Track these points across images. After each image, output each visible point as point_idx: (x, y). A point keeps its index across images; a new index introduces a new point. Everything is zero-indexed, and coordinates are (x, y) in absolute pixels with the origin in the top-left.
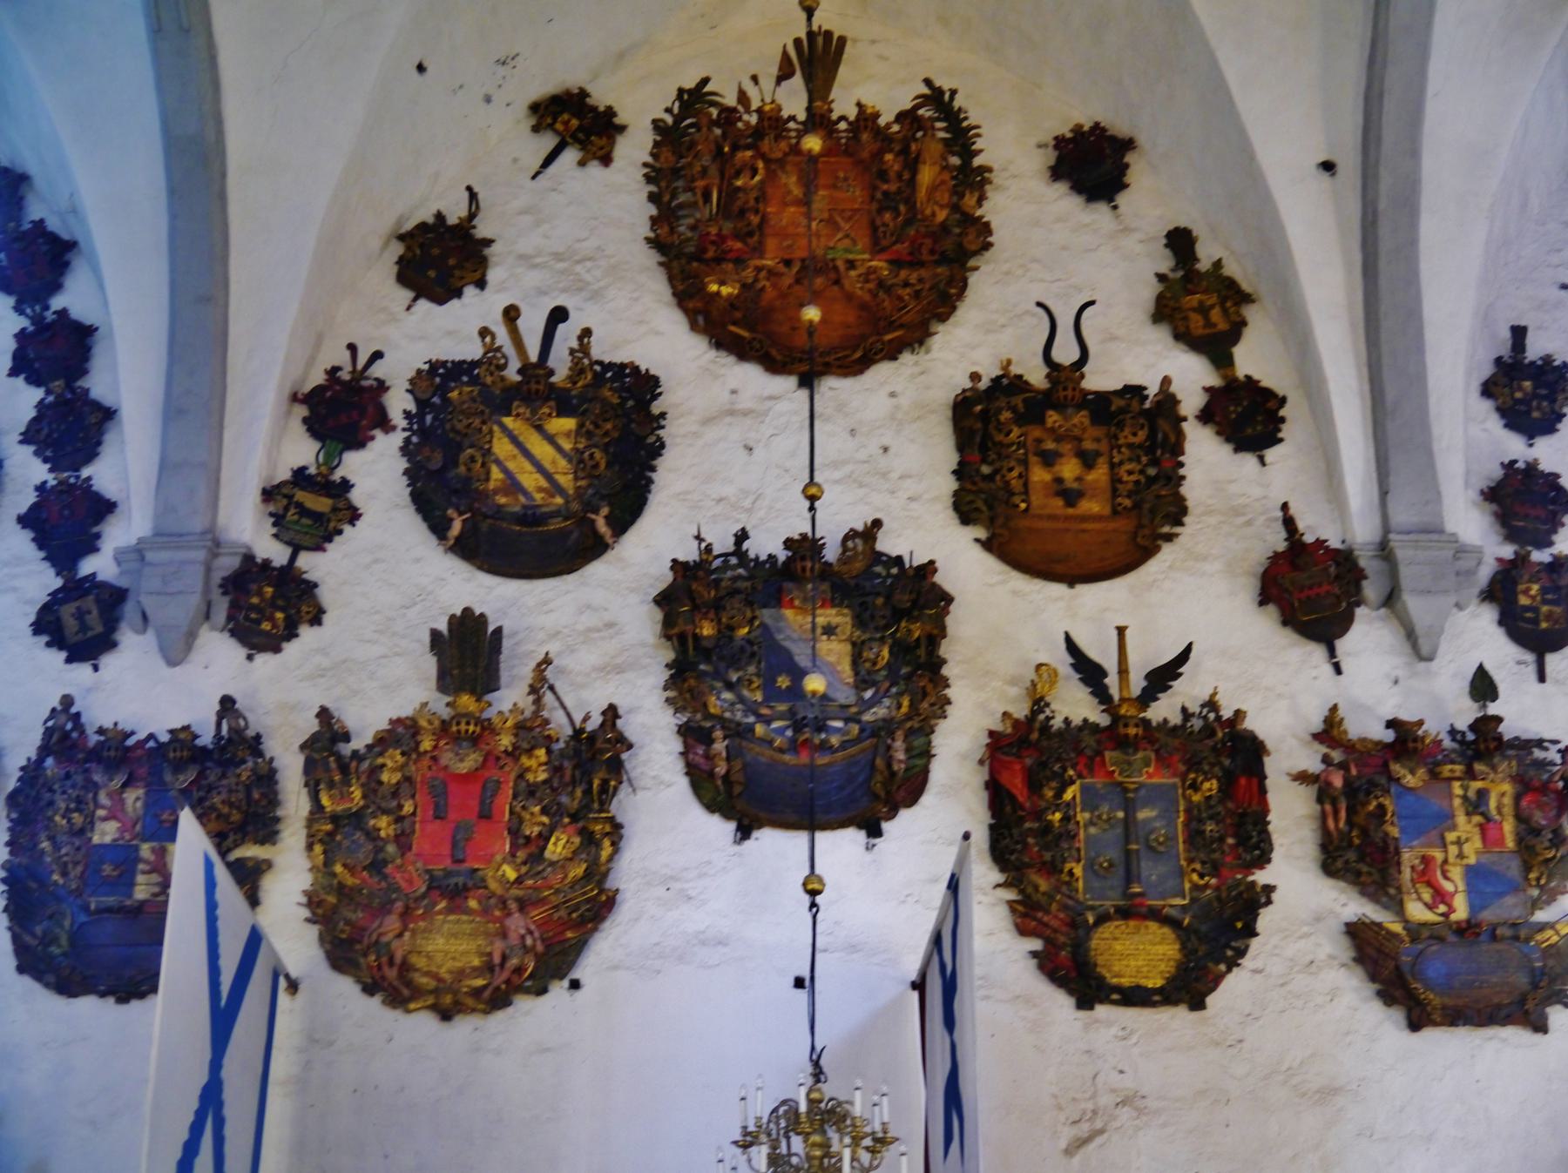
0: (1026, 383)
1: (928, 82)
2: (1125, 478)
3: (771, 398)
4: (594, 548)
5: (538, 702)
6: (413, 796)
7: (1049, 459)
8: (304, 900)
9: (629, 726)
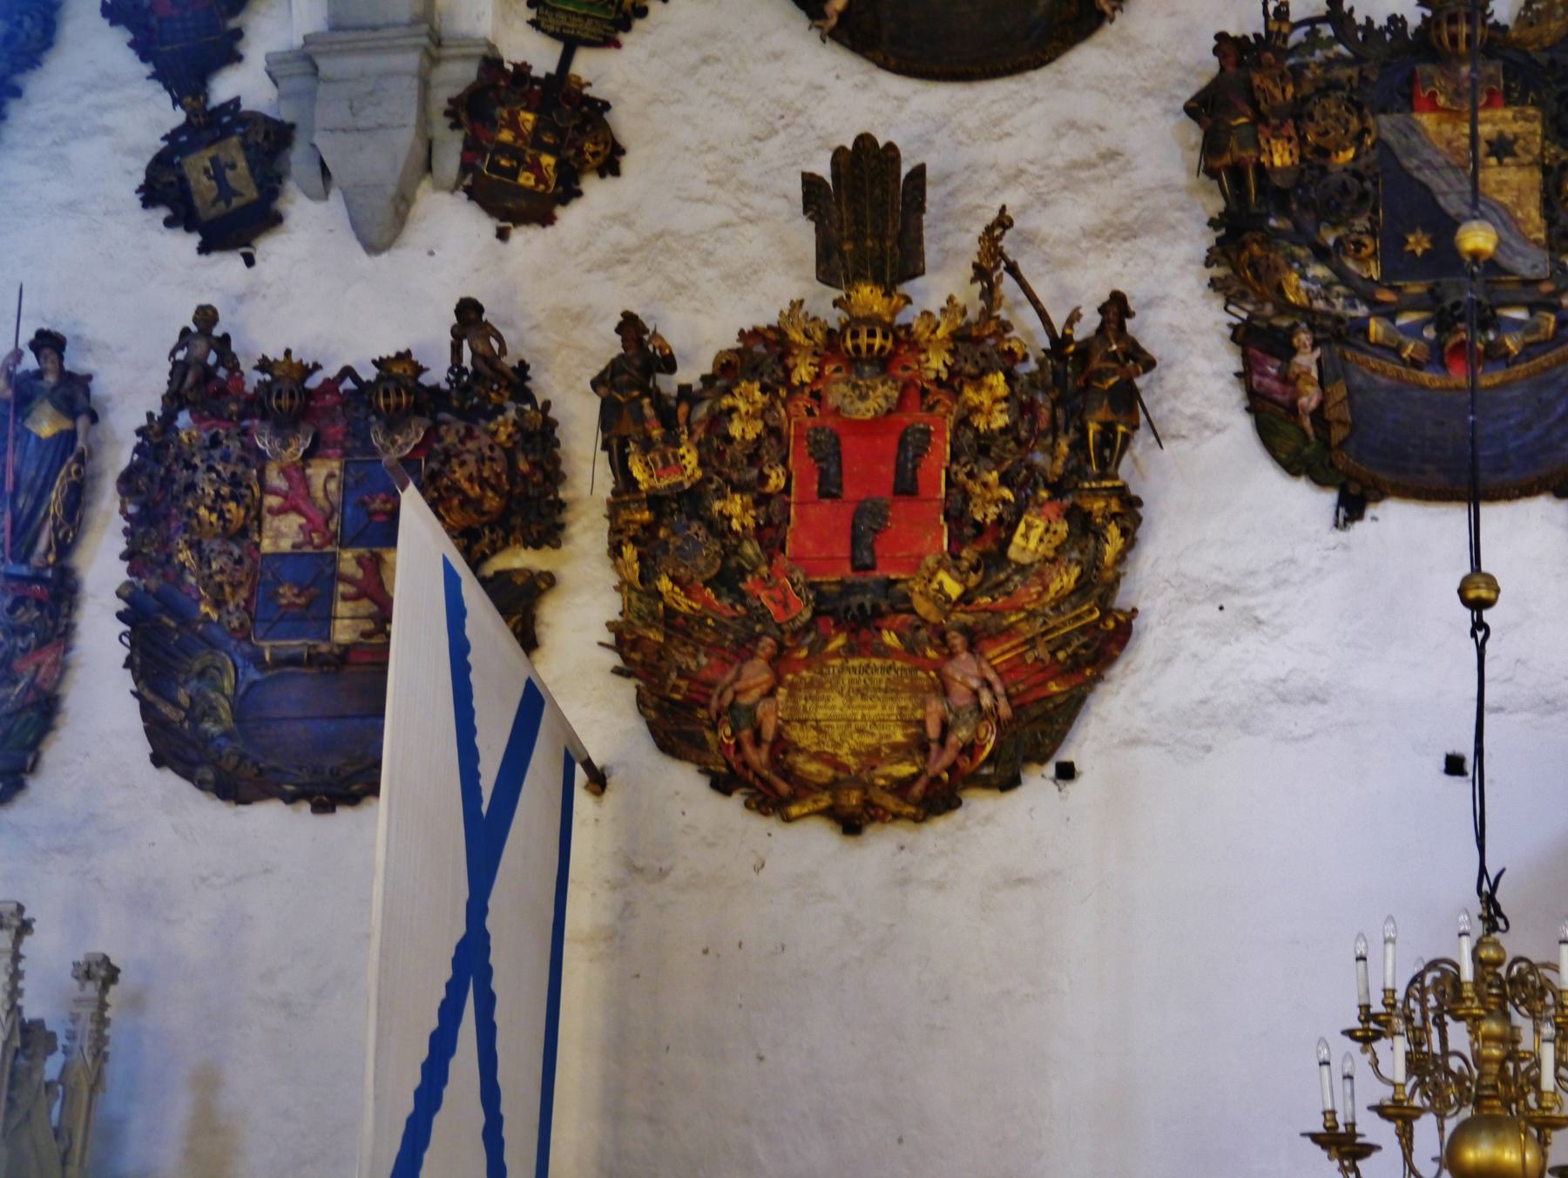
5: (990, 294)
6: (784, 462)
8: (610, 638)
9: (1147, 330)
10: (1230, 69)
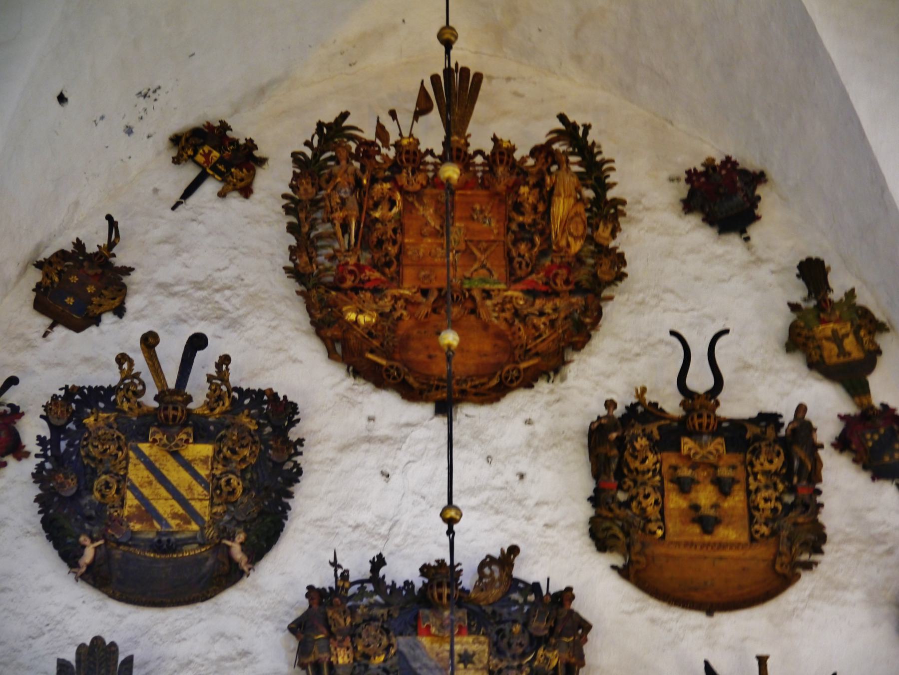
0: (662, 410)
1: (562, 118)
2: (762, 505)
3: (408, 425)
4: (228, 575)
7: (684, 486)
10: (315, 606)
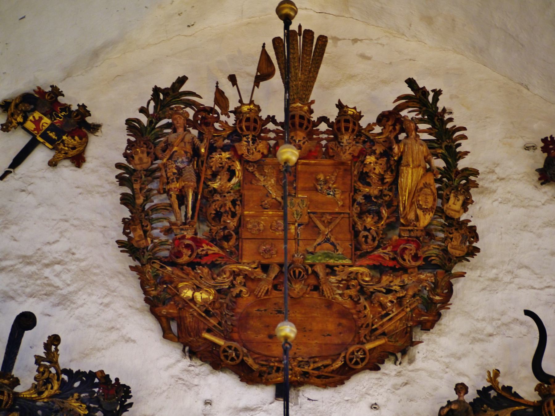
0: (516, 395)
1: (411, 83)
